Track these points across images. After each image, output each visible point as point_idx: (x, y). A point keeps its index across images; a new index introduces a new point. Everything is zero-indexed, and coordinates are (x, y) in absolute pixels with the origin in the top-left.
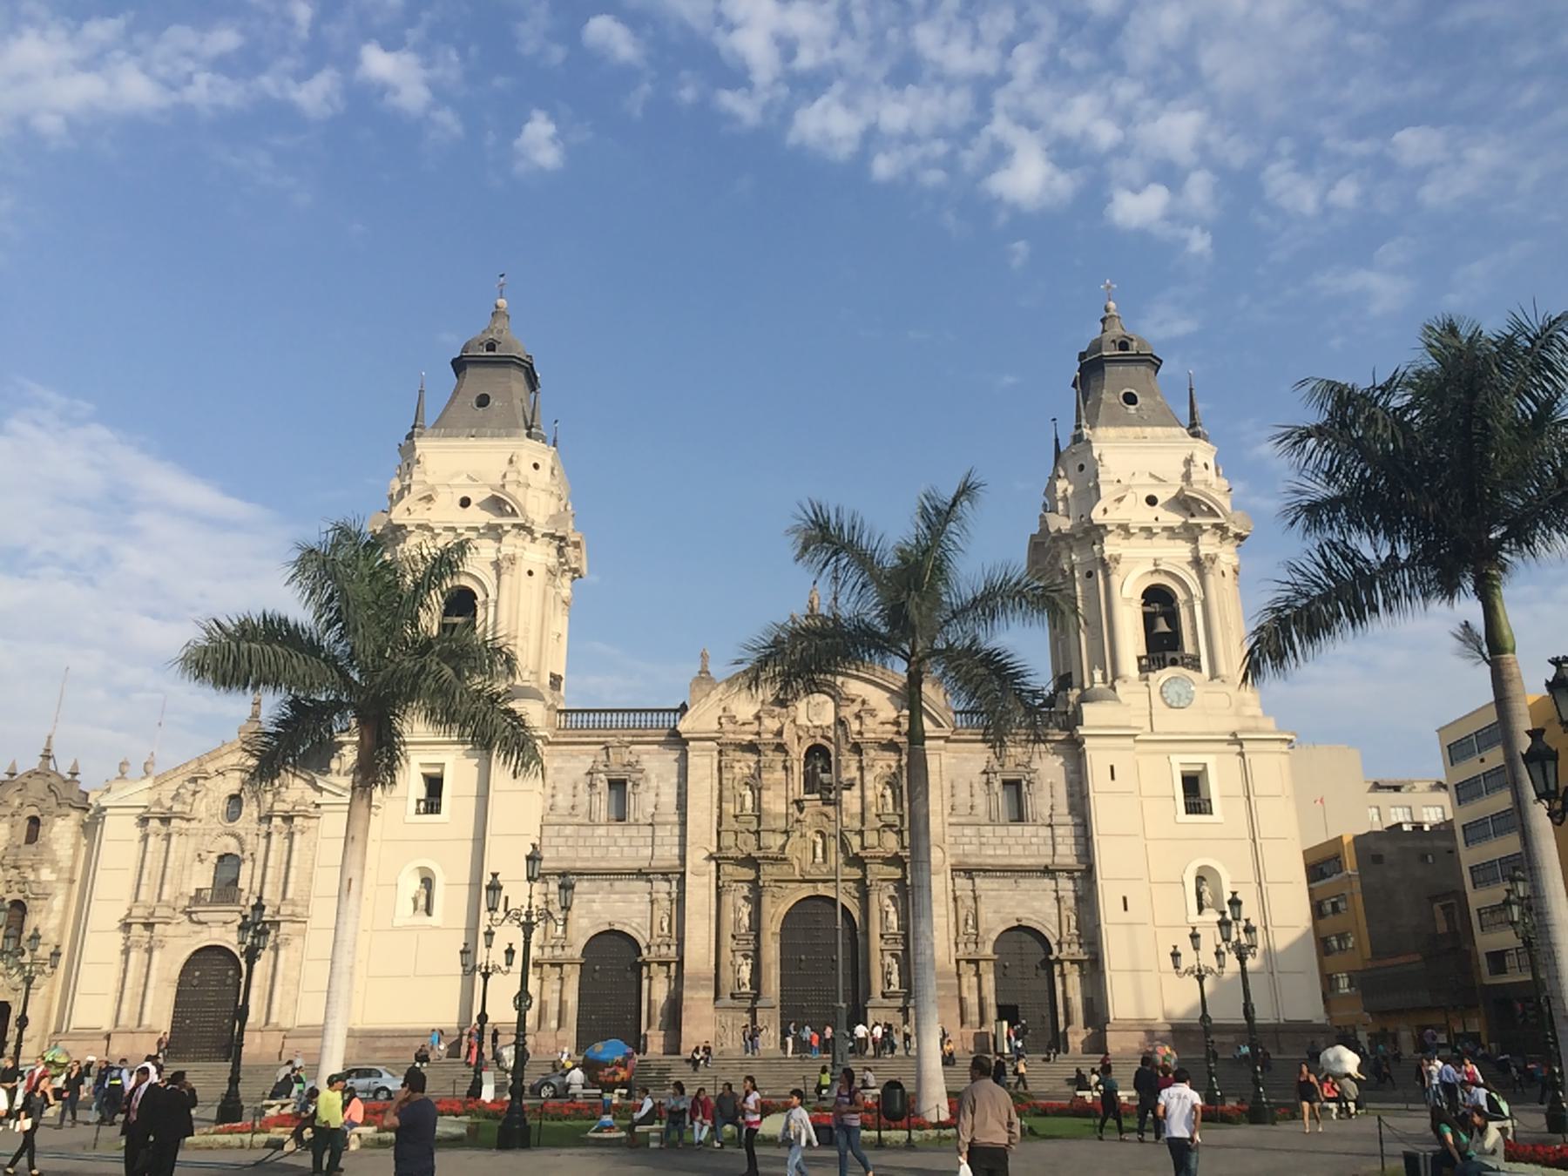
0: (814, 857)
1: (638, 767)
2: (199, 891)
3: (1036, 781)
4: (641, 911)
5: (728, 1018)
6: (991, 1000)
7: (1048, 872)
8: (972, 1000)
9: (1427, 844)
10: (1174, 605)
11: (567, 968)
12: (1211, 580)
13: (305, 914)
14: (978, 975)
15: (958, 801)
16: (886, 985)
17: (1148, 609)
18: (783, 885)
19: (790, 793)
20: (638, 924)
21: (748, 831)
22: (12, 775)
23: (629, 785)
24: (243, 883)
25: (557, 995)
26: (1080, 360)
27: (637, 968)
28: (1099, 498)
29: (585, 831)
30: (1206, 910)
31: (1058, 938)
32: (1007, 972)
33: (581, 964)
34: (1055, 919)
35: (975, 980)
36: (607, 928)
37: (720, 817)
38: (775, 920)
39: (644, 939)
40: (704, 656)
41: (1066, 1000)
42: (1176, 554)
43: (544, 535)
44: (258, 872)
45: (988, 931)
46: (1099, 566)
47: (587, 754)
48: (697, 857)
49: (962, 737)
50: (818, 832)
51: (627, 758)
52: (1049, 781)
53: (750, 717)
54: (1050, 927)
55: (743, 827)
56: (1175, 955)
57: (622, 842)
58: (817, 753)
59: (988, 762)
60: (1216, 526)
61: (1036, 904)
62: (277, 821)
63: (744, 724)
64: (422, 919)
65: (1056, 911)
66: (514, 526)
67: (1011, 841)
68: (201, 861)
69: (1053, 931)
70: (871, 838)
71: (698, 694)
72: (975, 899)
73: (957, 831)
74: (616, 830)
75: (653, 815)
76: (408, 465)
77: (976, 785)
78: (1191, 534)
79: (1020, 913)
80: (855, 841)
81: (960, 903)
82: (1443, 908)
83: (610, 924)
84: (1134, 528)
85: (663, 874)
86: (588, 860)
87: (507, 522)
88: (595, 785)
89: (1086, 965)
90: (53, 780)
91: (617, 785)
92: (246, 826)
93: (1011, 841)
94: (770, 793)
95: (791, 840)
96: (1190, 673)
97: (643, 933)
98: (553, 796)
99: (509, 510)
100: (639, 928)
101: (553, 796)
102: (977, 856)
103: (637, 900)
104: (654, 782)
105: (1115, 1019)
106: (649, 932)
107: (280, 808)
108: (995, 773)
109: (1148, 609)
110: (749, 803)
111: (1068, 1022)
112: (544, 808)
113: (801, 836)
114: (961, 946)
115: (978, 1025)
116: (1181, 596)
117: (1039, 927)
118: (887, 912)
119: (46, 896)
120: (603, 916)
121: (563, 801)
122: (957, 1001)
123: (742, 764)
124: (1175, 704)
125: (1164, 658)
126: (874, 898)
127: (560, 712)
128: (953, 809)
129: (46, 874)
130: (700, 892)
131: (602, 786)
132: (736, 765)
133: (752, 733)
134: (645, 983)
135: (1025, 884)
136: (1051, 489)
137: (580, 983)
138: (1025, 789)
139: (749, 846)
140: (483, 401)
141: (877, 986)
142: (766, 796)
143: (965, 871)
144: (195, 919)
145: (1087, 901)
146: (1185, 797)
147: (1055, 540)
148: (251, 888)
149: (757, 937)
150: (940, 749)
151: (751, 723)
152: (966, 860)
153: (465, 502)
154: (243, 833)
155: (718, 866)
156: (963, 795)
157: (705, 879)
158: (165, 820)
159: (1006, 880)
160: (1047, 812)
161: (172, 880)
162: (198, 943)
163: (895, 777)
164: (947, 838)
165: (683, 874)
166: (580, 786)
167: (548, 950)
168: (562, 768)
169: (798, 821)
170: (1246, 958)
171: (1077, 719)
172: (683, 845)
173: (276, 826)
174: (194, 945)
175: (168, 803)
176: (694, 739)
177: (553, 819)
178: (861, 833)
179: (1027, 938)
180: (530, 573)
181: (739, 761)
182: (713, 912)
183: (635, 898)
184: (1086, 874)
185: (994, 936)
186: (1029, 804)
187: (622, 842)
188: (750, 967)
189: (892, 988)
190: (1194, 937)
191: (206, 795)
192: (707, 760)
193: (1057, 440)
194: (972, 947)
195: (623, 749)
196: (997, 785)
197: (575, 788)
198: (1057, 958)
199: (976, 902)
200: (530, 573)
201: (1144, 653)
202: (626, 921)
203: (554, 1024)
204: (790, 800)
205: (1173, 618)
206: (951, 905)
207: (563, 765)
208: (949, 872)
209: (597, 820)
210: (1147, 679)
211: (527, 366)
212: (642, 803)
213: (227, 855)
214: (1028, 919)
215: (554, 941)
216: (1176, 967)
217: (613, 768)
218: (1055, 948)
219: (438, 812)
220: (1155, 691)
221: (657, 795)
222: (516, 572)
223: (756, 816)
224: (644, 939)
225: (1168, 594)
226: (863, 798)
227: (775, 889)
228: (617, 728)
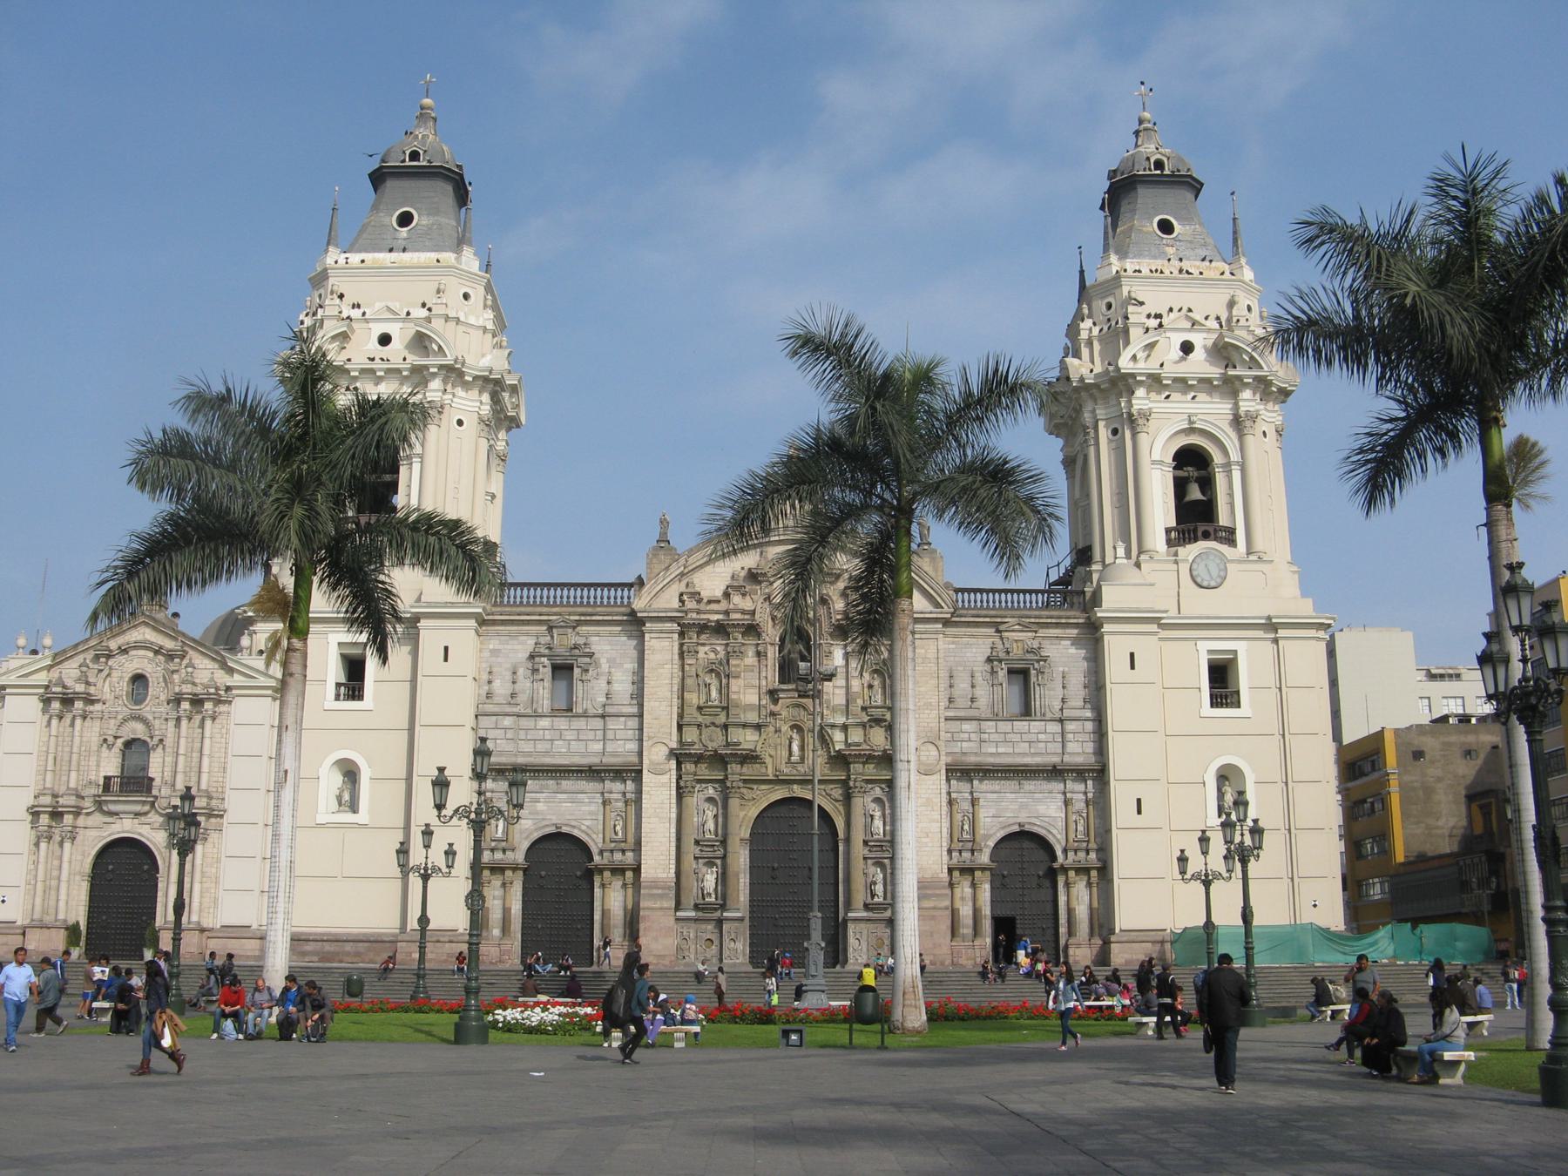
0: (790, 754)
1: (588, 650)
2: (107, 779)
3: (1046, 671)
4: (591, 813)
5: (691, 931)
6: (987, 911)
7: (1055, 772)
8: (966, 911)
10: (1209, 469)
11: (509, 873)
12: (1249, 439)
13: (221, 807)
14: (974, 886)
15: (956, 692)
16: (869, 895)
17: (1180, 473)
18: (755, 787)
19: (764, 683)
20: (588, 827)
21: (713, 724)
23: (577, 671)
26: (1110, 178)
27: (589, 875)
28: (1127, 343)
29: (524, 722)
31: (1064, 844)
33: (525, 871)
34: (1061, 824)
35: (968, 891)
36: (552, 830)
37: (682, 707)
38: (744, 824)
39: (596, 844)
40: (664, 523)
41: (1070, 911)
42: (1213, 412)
43: (476, 378)
44: (169, 759)
45: (987, 837)
46: (1126, 422)
47: (527, 634)
48: (656, 754)
49: (963, 619)
50: (792, 727)
51: (573, 638)
52: (1061, 669)
53: (718, 593)
54: (1055, 832)
55: (708, 720)
56: (1183, 860)
57: (569, 735)
59: (992, 648)
60: (1256, 378)
61: (1042, 809)
62: (185, 705)
63: (710, 602)
64: (349, 817)
65: (1064, 816)
66: (441, 367)
67: (1016, 738)
68: (110, 747)
69: (1059, 837)
71: (657, 568)
72: (974, 802)
73: (954, 726)
74: (562, 723)
76: (320, 296)
77: (977, 675)
78: (1230, 387)
79: (1023, 817)
80: (838, 736)
81: (955, 807)
82: (1481, 807)
83: (557, 828)
84: (1167, 378)
85: (617, 772)
86: (529, 754)
87: (433, 361)
88: (538, 670)
91: (562, 670)
92: (153, 709)
93: (1016, 738)
94: (741, 682)
95: (764, 736)
96: (1224, 548)
97: (594, 836)
98: (490, 682)
99: (436, 348)
100: (590, 832)
101: (490, 682)
104: (605, 667)
105: (1121, 930)
106: (601, 836)
107: (190, 691)
108: (1000, 661)
109: (1180, 473)
110: (714, 694)
111: (1070, 933)
113: (776, 731)
114: (955, 854)
115: (971, 937)
116: (1217, 458)
117: (1042, 832)
118: (872, 816)
120: (548, 817)
121: (501, 687)
122: (948, 913)
123: (707, 648)
124: (1205, 584)
125: (1195, 531)
126: (858, 802)
128: (950, 702)
130: (659, 791)
131: (549, 669)
132: (702, 650)
133: (717, 612)
134: (598, 892)
135: (1029, 785)
136: (1073, 331)
137: (524, 888)
138: (1033, 679)
139: (714, 740)
140: (405, 219)
141: (860, 897)
143: (962, 771)
144: (105, 808)
145: (1101, 804)
146: (1211, 688)
147: (1076, 389)
148: (163, 777)
149: (724, 842)
150: (937, 632)
151: (718, 602)
152: (963, 758)
154: (150, 717)
155: (679, 764)
156: (962, 686)
157: (665, 778)
158: (67, 701)
159: (1009, 782)
160: (1057, 705)
161: (79, 765)
162: (110, 835)
163: (885, 664)
164: (942, 734)
165: (640, 771)
166: (521, 672)
168: (499, 650)
169: (773, 714)
170: (1249, 861)
171: (1096, 599)
172: (641, 740)
173: (185, 710)
174: (105, 838)
175: (69, 682)
176: (653, 619)
177: (490, 708)
178: (845, 728)
179: (1027, 844)
180: (460, 423)
181: (703, 645)
182: (674, 816)
184: (1099, 773)
185: (991, 844)
186: (1037, 696)
187: (569, 735)
188: (715, 876)
189: (876, 899)
191: (109, 675)
192: (666, 643)
193: (1082, 272)
194: (966, 855)
195: (570, 630)
196: (1002, 674)
197: (514, 673)
198: (1062, 865)
199: (973, 806)
200: (460, 423)
201: (1173, 524)
202: (573, 823)
203: (496, 932)
204: (764, 690)
205: (1207, 484)
206: (945, 809)
207: (497, 647)
208: (944, 772)
209: (540, 711)
210: (1176, 554)
211: (457, 177)
212: (591, 692)
213: (134, 740)
214: (1030, 823)
215: (493, 844)
216: (1183, 872)
217: (560, 650)
218: (1059, 853)
219: (360, 697)
221: (609, 683)
222: (444, 423)
223: (723, 708)
224: (596, 844)
225: (1203, 456)
226: (847, 687)
227: (744, 791)
228: (562, 605)
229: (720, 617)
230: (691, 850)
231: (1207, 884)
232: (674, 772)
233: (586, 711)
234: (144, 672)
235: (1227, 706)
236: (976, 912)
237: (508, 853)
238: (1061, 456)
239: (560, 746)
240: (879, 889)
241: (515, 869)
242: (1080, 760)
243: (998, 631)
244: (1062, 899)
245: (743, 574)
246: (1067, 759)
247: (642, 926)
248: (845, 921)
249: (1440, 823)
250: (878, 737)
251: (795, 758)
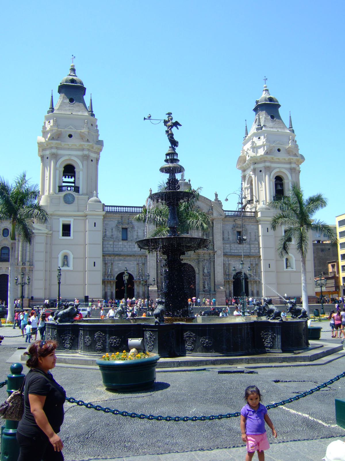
4: (133, 267)
6: (232, 291)
9: (323, 247)
23: (128, 230)
29: (115, 243)
40: (151, 191)
41: (252, 292)
67: (239, 248)
74: (125, 243)
75: (136, 239)
77: (229, 232)
82: (332, 265)
86: (117, 252)
91: (125, 230)
98: (105, 232)
102: (229, 252)
103: (132, 264)
104: (136, 229)
106: (136, 273)
109: (277, 182)
112: (103, 236)
126: (201, 264)
131: (121, 229)
153: (70, 136)
166: (114, 229)
177: (106, 238)
180: (92, 161)
183: (131, 263)
187: (127, 247)
194: (227, 277)
196: (236, 232)
200: (92, 161)
205: (282, 185)
219: (70, 236)
221: (137, 233)
232: (156, 256)
233: (132, 240)
234: (7, 228)
236: (230, 292)
238: (241, 175)
239: (125, 250)
240: (206, 286)
242: (254, 254)
244: (250, 289)
246: (251, 254)
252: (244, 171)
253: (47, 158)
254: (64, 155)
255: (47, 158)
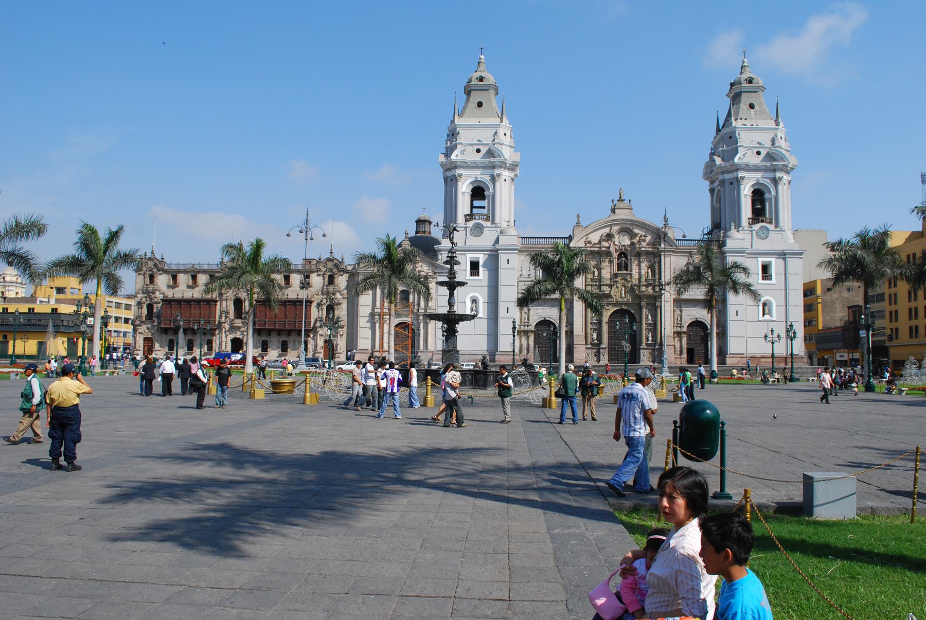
0: (621, 295)
5: (590, 351)
22: (320, 259)
24: (411, 299)
25: (526, 342)
28: (737, 153)
30: (766, 316)
32: (691, 337)
40: (578, 216)
45: (685, 322)
55: (594, 284)
58: (622, 254)
63: (594, 244)
70: (643, 289)
82: (852, 311)
89: (721, 335)
90: (335, 261)
94: (605, 270)
110: (596, 274)
117: (704, 321)
119: (340, 304)
125: (758, 219)
127: (522, 238)
129: (338, 295)
140: (480, 105)
142: (603, 272)
167: (522, 327)
180: (505, 180)
182: (584, 314)
185: (687, 324)
190: (772, 331)
193: (718, 119)
200: (505, 180)
203: (526, 352)
205: (763, 202)
216: (766, 340)
220: (754, 233)
229: (597, 249)
230: (589, 326)
231: (773, 343)
235: (767, 279)
237: (530, 327)
241: (531, 331)
243: (690, 254)
245: (605, 234)
247: (575, 350)
248: (639, 350)
249: (836, 315)
250: (650, 290)
251: (623, 296)
252: (712, 182)
253: (452, 180)
254: (470, 176)
255: (452, 180)
